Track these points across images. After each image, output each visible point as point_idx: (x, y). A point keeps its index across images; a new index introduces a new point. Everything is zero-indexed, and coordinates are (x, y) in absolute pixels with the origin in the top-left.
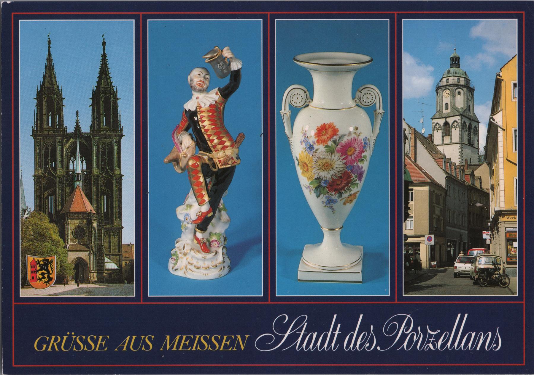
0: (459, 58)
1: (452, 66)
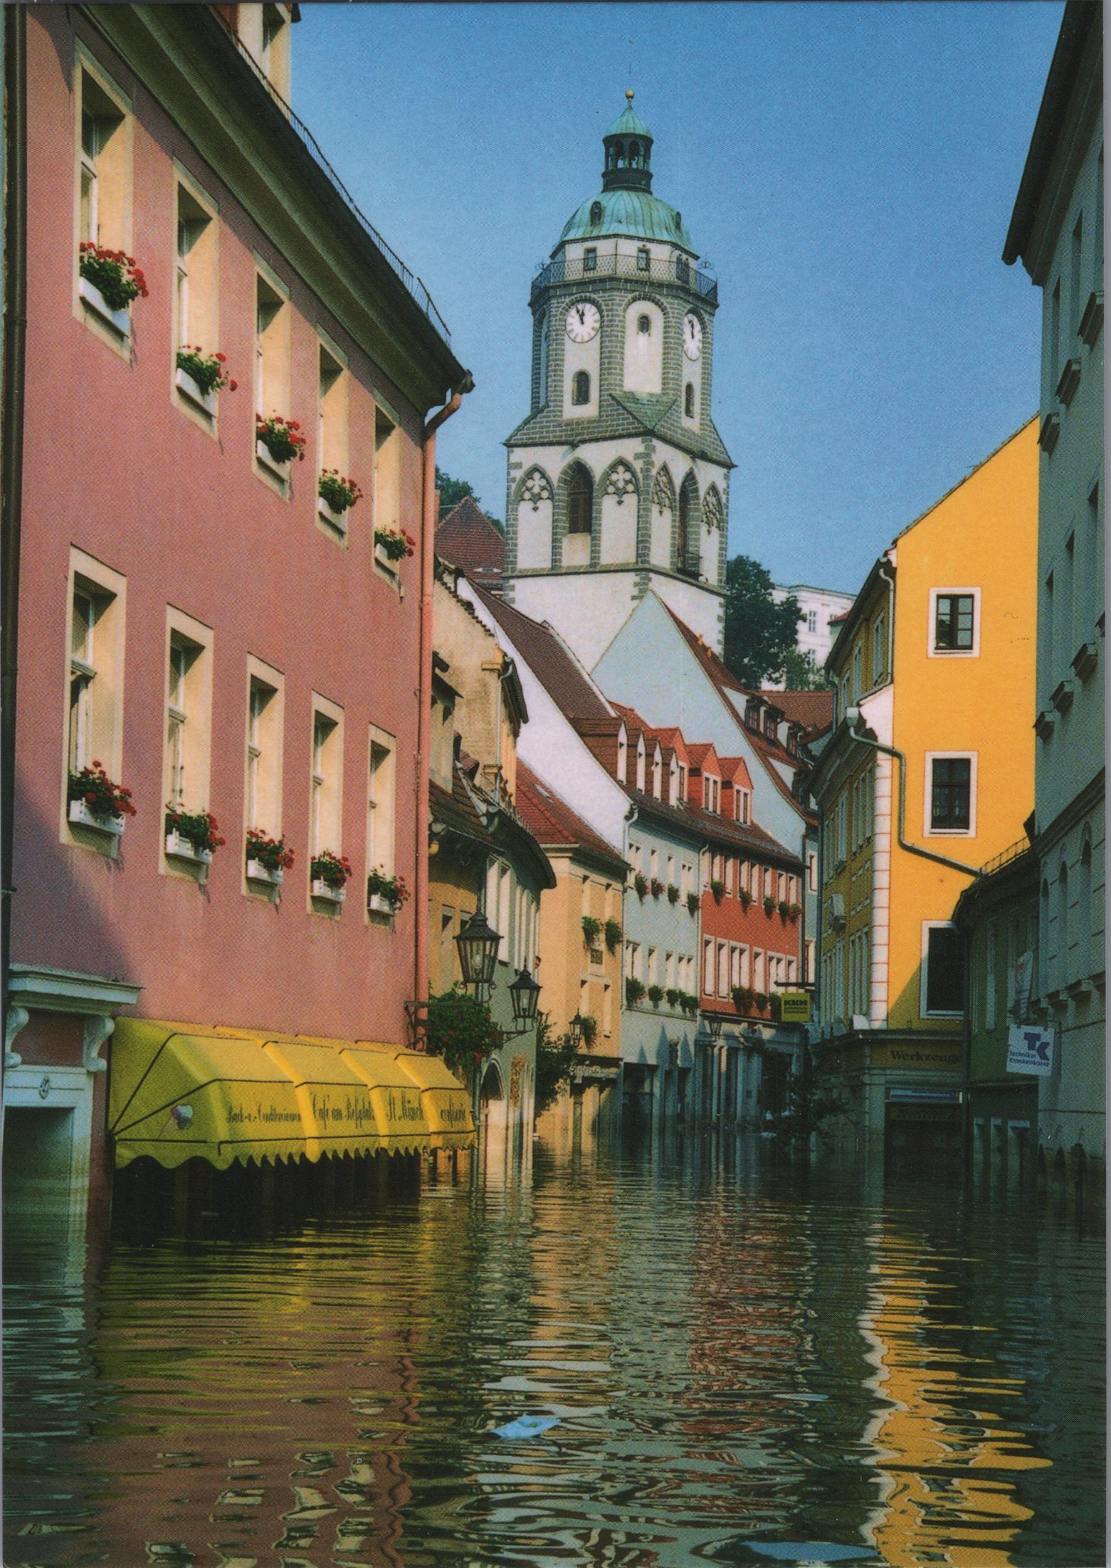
0: (648, 141)
1: (613, 180)
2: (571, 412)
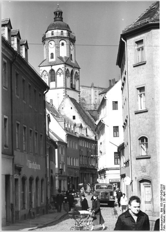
2: (51, 60)
